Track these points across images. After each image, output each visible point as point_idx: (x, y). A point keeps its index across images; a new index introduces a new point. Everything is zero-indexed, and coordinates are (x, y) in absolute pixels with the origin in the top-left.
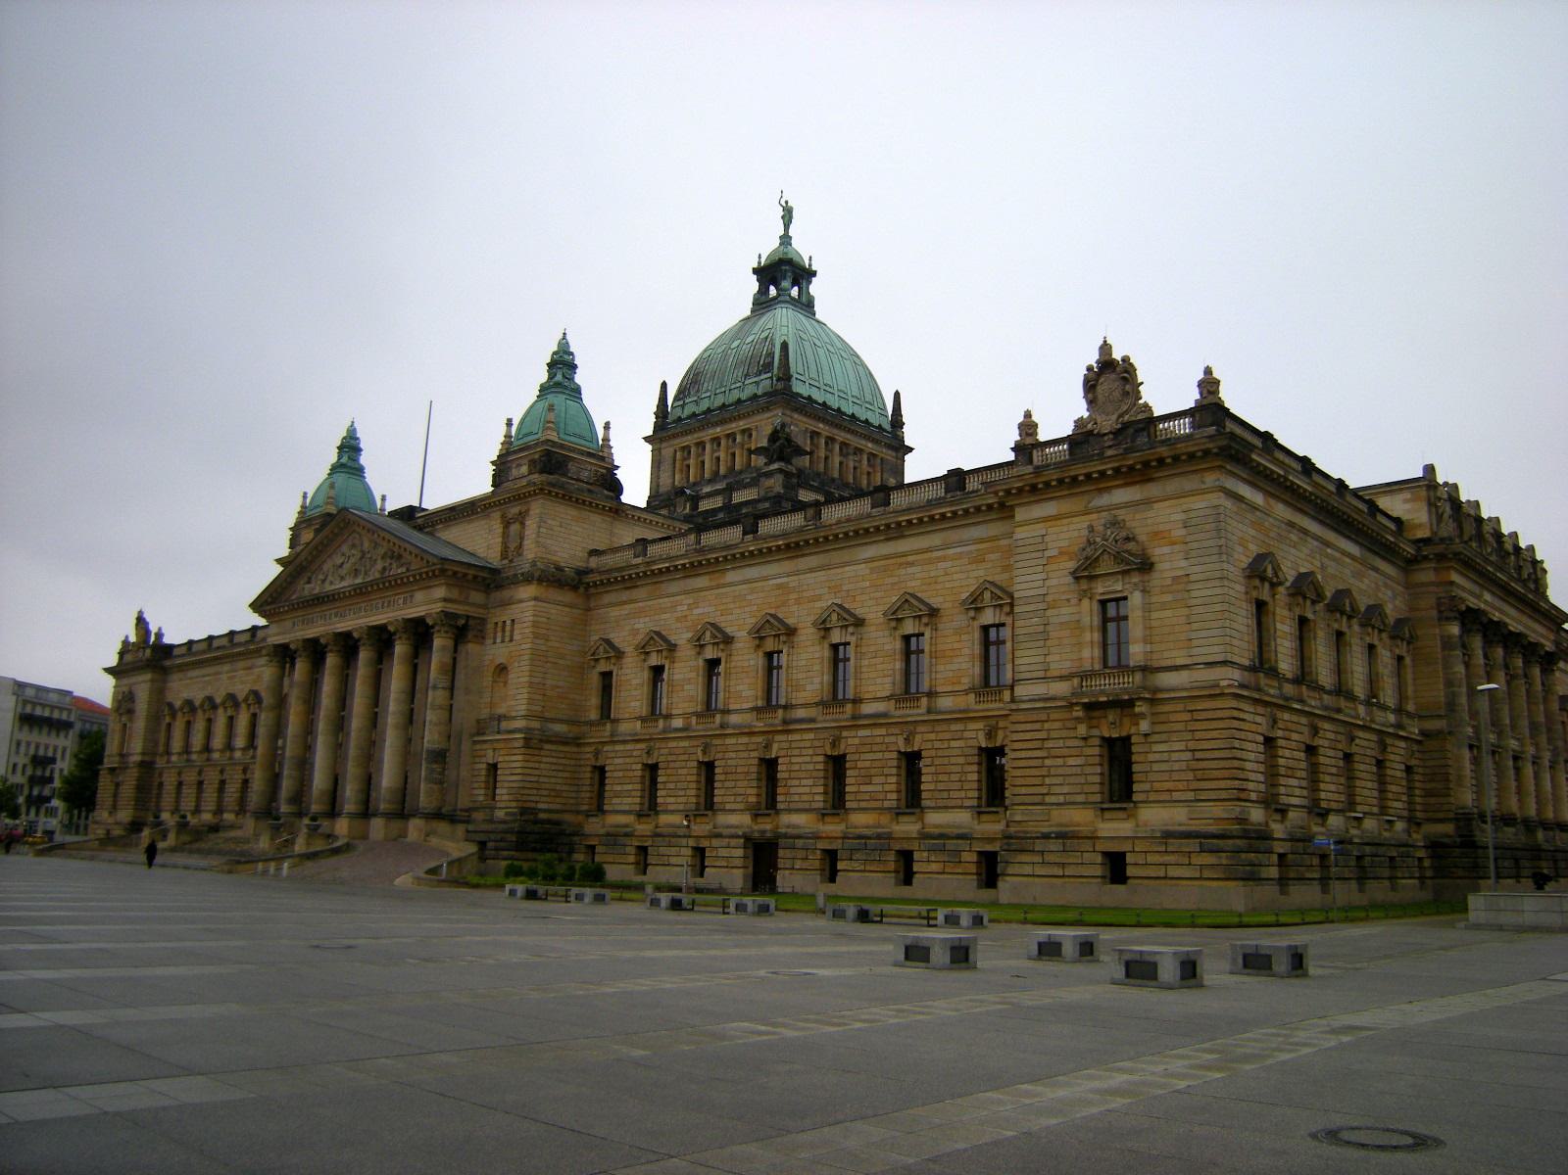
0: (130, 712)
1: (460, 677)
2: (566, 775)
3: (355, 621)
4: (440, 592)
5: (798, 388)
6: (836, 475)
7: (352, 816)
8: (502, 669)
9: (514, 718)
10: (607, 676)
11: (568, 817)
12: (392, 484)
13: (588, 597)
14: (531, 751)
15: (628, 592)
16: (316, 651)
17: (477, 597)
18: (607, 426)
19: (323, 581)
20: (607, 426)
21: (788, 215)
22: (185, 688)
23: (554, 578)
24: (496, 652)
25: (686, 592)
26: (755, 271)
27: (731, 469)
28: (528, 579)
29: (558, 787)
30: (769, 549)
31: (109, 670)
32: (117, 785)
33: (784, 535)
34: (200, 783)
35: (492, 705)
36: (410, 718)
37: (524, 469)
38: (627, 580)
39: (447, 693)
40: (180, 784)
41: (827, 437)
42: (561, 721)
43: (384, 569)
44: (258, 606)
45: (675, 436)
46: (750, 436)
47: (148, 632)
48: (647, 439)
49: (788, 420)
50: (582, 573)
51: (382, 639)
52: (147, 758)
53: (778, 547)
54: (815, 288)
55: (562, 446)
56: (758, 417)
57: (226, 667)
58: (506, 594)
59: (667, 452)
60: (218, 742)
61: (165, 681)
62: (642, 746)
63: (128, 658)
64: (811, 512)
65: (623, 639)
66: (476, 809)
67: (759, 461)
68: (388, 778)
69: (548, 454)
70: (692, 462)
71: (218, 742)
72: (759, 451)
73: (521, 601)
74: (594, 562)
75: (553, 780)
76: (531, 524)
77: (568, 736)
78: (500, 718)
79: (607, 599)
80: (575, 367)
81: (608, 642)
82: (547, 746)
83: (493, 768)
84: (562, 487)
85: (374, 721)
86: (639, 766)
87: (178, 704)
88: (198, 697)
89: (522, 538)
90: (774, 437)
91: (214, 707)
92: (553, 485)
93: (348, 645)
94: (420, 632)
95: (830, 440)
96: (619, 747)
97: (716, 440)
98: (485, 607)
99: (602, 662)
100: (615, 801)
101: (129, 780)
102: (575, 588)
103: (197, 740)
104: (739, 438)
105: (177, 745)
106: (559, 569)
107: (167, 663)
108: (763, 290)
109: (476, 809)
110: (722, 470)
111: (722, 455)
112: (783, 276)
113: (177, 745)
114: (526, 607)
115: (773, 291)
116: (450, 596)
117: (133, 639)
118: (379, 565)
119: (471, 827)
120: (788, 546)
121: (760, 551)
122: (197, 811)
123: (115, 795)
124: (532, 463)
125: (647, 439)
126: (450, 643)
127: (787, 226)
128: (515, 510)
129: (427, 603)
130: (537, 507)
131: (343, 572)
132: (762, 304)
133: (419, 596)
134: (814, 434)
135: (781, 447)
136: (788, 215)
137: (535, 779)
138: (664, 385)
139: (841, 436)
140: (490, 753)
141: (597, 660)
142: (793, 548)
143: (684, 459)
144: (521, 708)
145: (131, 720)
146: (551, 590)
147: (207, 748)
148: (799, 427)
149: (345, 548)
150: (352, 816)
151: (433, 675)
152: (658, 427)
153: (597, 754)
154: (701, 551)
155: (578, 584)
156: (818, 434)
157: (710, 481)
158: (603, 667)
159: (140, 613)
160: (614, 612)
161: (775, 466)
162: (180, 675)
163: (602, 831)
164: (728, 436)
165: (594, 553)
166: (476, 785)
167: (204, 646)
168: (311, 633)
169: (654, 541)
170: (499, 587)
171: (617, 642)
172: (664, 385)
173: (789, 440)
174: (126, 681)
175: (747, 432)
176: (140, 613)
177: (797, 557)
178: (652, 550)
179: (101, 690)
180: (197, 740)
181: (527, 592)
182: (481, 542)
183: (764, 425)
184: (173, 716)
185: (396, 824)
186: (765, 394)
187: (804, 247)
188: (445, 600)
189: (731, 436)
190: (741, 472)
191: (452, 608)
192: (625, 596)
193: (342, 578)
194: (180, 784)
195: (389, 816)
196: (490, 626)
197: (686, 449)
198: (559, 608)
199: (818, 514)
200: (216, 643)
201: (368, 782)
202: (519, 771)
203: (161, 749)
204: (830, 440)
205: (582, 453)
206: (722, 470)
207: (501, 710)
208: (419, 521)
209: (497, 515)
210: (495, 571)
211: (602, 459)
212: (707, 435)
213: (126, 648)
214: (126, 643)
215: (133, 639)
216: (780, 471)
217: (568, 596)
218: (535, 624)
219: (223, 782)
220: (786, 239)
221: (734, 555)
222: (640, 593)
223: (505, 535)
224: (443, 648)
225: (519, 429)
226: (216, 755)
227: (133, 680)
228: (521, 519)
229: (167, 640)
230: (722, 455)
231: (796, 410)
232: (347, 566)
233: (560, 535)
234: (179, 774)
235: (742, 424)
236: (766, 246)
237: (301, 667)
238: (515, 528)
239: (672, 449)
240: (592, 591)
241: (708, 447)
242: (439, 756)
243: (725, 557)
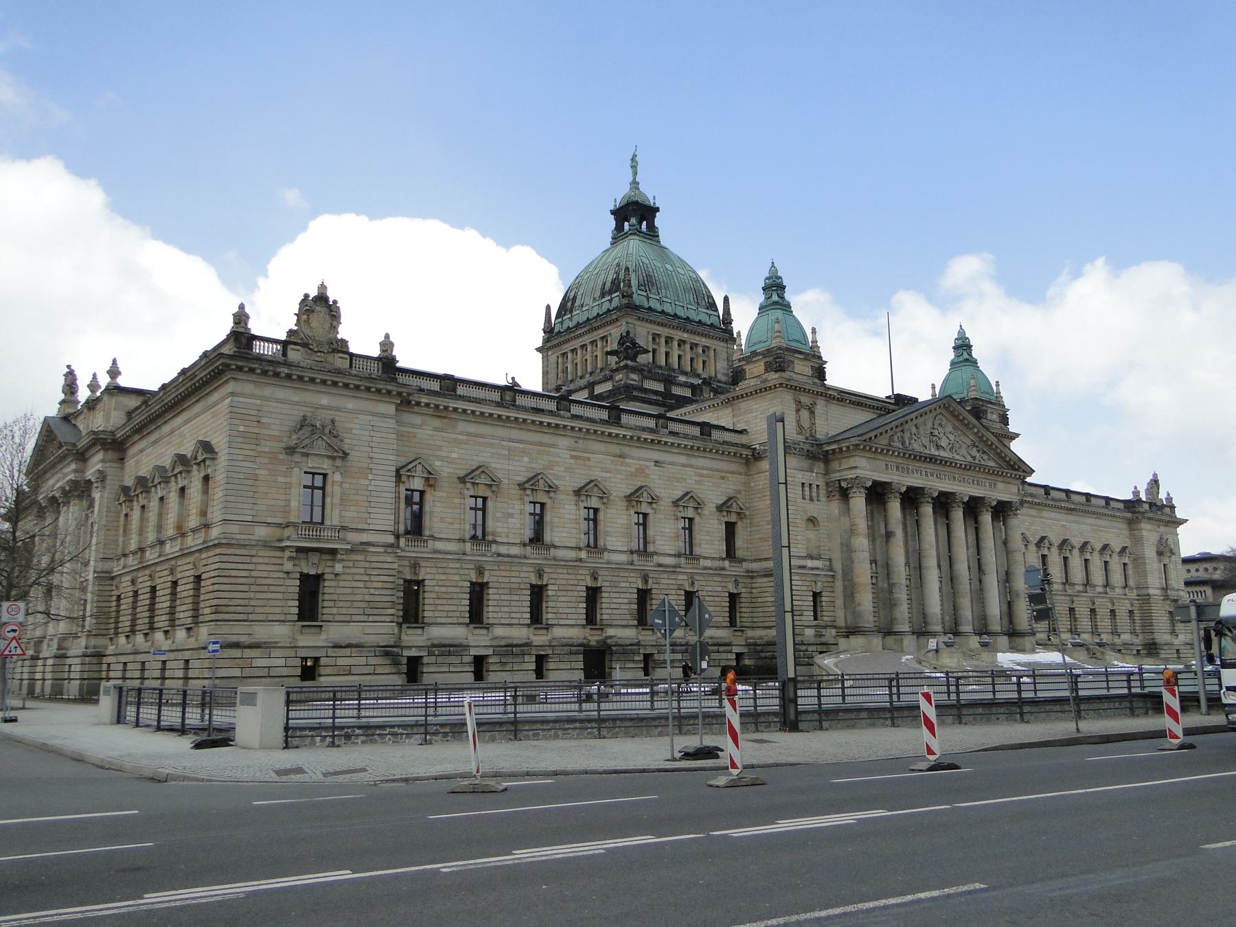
6: (663, 363)
26: (613, 212)
48: (538, 350)
59: (553, 359)
90: (622, 342)
108: (619, 227)
112: (635, 215)
125: (538, 350)
135: (629, 348)
138: (548, 308)
148: (642, 333)
152: (546, 341)
172: (548, 308)
173: (634, 344)
187: (650, 192)
220: (635, 184)
236: (618, 193)
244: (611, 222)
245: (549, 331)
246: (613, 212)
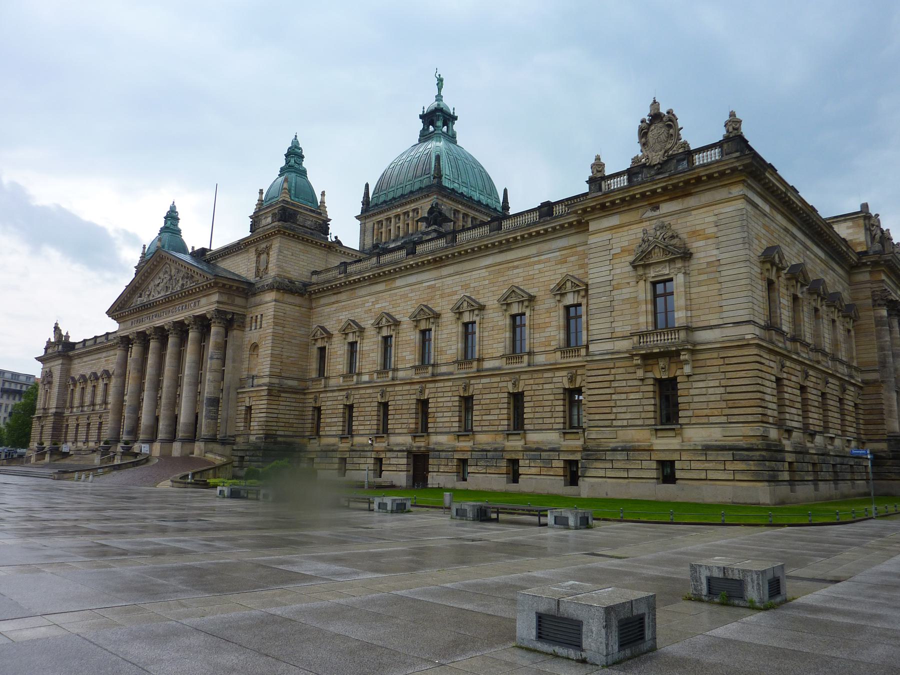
0: (50, 383)
1: (229, 352)
2: (297, 413)
4: (215, 298)
5: (446, 183)
7: (163, 441)
9: (262, 377)
10: (322, 350)
11: (298, 440)
12: (195, 236)
13: (311, 300)
14: (272, 398)
15: (335, 296)
16: (143, 338)
17: (239, 301)
18: (323, 194)
19: (149, 295)
20: (323, 194)
21: (440, 82)
22: (81, 368)
24: (251, 335)
25: (370, 294)
26: (421, 117)
27: (407, 234)
28: (271, 288)
29: (291, 421)
30: (423, 262)
31: (38, 359)
32: (42, 426)
33: (432, 252)
34: (89, 424)
35: (249, 369)
36: (198, 381)
37: (269, 220)
38: (335, 289)
39: (219, 361)
40: (78, 425)
41: (464, 214)
42: (293, 379)
43: (183, 285)
44: (115, 312)
45: (374, 215)
46: (418, 213)
47: (61, 335)
48: (357, 217)
49: (440, 202)
50: (306, 285)
51: (181, 329)
52: (59, 410)
53: (429, 261)
54: (457, 127)
55: (293, 205)
56: (423, 201)
57: (104, 354)
58: (257, 299)
59: (369, 225)
60: (99, 400)
61: (70, 365)
62: (344, 393)
63: (50, 351)
64: (449, 237)
65: (333, 326)
66: (239, 435)
67: (422, 226)
68: (184, 417)
69: (283, 209)
70: (383, 230)
71: (99, 400)
72: (422, 219)
73: (267, 303)
74: (314, 279)
75: (287, 416)
76: (273, 254)
78: (253, 377)
79: (323, 301)
80: (303, 157)
81: (323, 328)
82: (283, 395)
83: (249, 409)
84: (293, 230)
85: (177, 383)
86: (342, 406)
87: (77, 377)
88: (87, 372)
89: (268, 263)
90: (431, 211)
91: (97, 378)
92: (286, 228)
93: (162, 334)
94: (204, 324)
95: (465, 215)
96: (329, 395)
97: (397, 216)
98: (245, 307)
99: (320, 341)
100: (326, 429)
101: (49, 423)
102: (301, 295)
103: (88, 399)
104: (411, 214)
105: (76, 402)
106: (291, 282)
107: (71, 353)
109: (239, 435)
110: (401, 235)
111: (401, 225)
112: (438, 120)
113: (76, 402)
115: (431, 128)
116: (221, 300)
117: (53, 340)
118: (181, 282)
119: (235, 447)
120: (435, 260)
121: (417, 264)
122: (86, 441)
123: (41, 433)
124: (274, 215)
125: (357, 217)
126: (222, 330)
127: (440, 90)
128: (264, 246)
129: (207, 305)
130: (276, 243)
131: (159, 289)
132: (425, 136)
133: (203, 301)
134: (456, 212)
135: (436, 217)
136: (440, 82)
137: (275, 415)
138: (367, 186)
139: (472, 213)
140: (247, 399)
141: (316, 340)
142: (438, 262)
143: (378, 229)
144: (266, 370)
145: (50, 388)
146: (286, 296)
147: (93, 404)
149: (161, 275)
150: (163, 441)
151: (210, 350)
152: (364, 211)
153: (315, 400)
154: (380, 266)
156: (458, 211)
157: (394, 241)
158: (320, 344)
159: (56, 324)
160: (327, 310)
161: (433, 227)
162: (79, 360)
163: (319, 449)
164: (405, 213)
165: (315, 273)
166: (238, 420)
167: (92, 342)
168: (141, 328)
169: (351, 263)
170: (254, 294)
171: (328, 328)
172: (367, 186)
173: (440, 213)
174: (48, 365)
175: (415, 210)
176: (56, 324)
177: (441, 267)
178: (350, 269)
179: (36, 370)
180: (88, 399)
181: (270, 296)
182: (243, 267)
183: (425, 206)
184: (75, 385)
185: (188, 446)
186: (426, 187)
187: (450, 103)
188: (218, 302)
189: (406, 214)
190: (412, 235)
192: (334, 298)
193: (159, 293)
194: (78, 425)
195: (184, 441)
196: (248, 319)
197: (380, 222)
198: (292, 306)
199: (454, 239)
200: (98, 340)
201: (175, 419)
202: (265, 410)
203: (68, 405)
204: (465, 215)
205: (306, 210)
206: (401, 235)
207: (254, 373)
208: (208, 257)
209: (253, 250)
210: (250, 284)
211: (320, 214)
212: (392, 213)
213: (49, 345)
214: (49, 342)
215: (53, 340)
216: (435, 230)
217: (297, 300)
218: (275, 317)
219: (101, 423)
221: (400, 268)
222: (343, 296)
223: (258, 262)
224: (217, 333)
225: (267, 195)
226: (97, 407)
227: (52, 364)
228: (267, 251)
229: (71, 340)
230: (401, 225)
231: (444, 196)
232: (161, 285)
233: (289, 260)
234: (77, 419)
235: (413, 206)
237: (135, 350)
238: (263, 257)
239: (372, 223)
240: (314, 296)
241: (393, 220)
243: (395, 270)
244: (420, 125)
245: (366, 202)
246: (421, 117)
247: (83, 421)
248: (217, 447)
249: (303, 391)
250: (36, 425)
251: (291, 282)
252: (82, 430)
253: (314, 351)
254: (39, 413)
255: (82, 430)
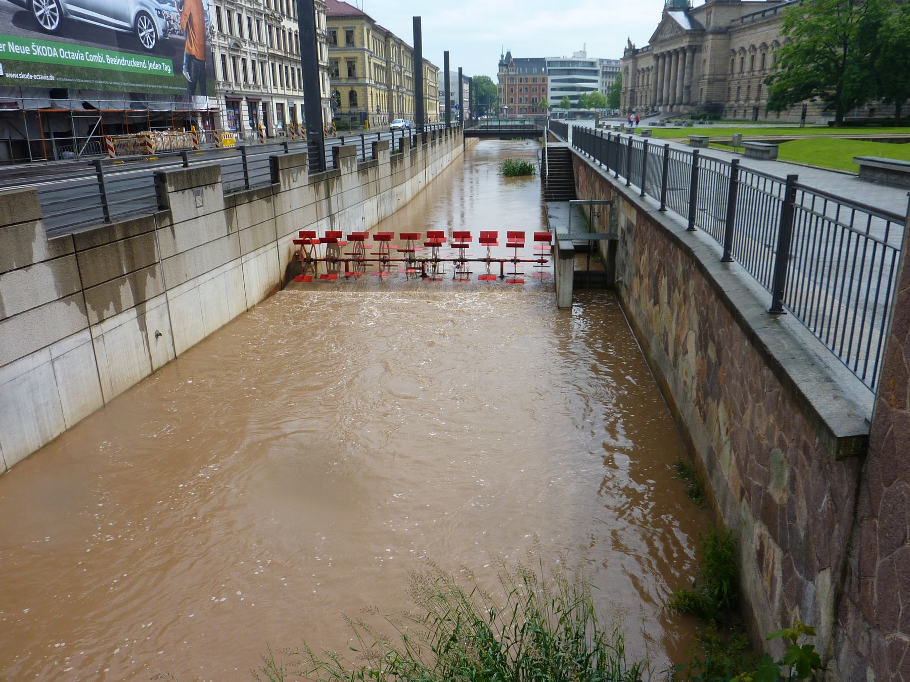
3: (670, 48)
8: (705, 61)
17: (699, 39)
23: (718, 32)
50: (728, 28)
74: (733, 24)
77: (720, 79)
94: (683, 50)
114: (709, 42)
155: (726, 32)
160: (736, 40)
165: (733, 21)
181: (710, 37)
191: (691, 44)
198: (720, 40)
217: (723, 36)
228: (710, 12)
242: (688, 87)
247: (644, 94)
248: (689, 107)
249: (725, 80)
250: (622, 96)
251: (720, 28)
252: (644, 98)
253: (730, 61)
254: (623, 90)
255: (644, 98)
